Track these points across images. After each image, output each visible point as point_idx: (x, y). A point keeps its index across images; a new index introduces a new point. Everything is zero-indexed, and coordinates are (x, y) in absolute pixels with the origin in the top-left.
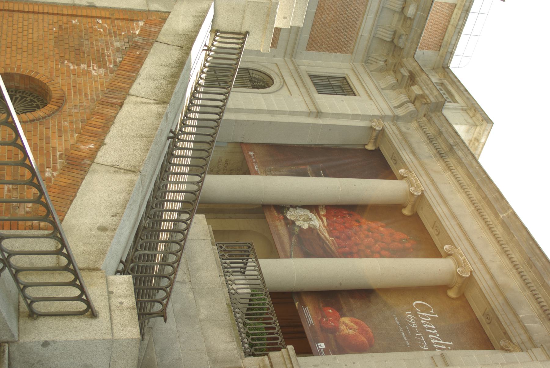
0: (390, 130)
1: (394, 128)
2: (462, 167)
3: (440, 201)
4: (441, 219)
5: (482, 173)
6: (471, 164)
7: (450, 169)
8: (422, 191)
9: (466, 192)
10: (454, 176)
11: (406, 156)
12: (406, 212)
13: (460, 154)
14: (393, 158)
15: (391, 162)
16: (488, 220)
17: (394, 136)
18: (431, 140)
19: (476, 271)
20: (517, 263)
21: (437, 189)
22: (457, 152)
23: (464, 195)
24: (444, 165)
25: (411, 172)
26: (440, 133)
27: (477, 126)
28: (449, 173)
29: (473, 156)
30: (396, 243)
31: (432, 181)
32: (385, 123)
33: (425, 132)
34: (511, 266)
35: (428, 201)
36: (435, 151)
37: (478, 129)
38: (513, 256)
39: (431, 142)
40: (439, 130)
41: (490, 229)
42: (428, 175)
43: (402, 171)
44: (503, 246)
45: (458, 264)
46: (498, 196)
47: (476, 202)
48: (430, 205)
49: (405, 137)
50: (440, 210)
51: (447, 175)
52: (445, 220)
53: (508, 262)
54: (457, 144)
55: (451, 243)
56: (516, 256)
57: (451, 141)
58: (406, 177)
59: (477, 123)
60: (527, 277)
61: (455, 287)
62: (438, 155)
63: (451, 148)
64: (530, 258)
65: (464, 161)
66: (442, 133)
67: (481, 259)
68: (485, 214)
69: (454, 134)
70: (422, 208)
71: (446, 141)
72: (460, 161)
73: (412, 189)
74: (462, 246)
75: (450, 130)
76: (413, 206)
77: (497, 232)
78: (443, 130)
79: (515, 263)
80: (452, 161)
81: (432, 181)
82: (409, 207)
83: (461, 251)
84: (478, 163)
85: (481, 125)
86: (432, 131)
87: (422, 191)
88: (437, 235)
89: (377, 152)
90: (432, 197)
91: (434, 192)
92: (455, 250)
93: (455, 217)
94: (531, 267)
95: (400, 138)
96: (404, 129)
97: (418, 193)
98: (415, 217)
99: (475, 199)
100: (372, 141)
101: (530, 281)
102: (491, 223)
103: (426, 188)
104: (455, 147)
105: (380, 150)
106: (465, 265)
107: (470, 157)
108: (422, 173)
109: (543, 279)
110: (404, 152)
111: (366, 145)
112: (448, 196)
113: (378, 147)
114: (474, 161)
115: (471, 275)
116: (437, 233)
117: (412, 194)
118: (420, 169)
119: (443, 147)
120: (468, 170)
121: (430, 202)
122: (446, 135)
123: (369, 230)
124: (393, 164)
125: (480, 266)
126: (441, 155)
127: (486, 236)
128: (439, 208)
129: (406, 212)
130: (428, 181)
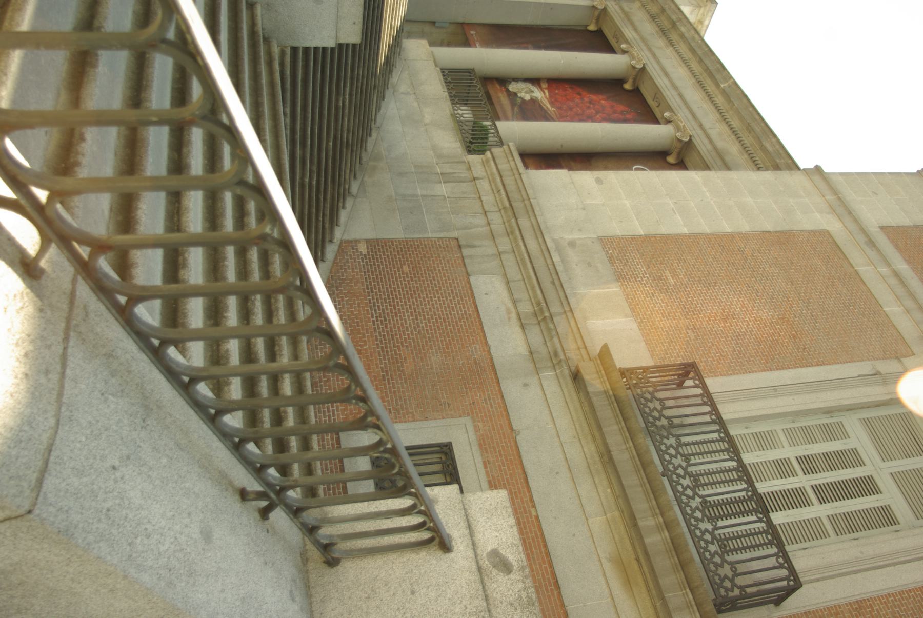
0: (613, 9)
1: (617, 7)
2: (684, 42)
3: (661, 73)
4: (662, 90)
5: (704, 47)
6: (693, 38)
7: (671, 44)
8: (644, 64)
9: (687, 66)
10: (676, 51)
11: (628, 33)
12: (627, 86)
13: (683, 29)
14: (615, 37)
15: (613, 42)
16: (709, 91)
17: (616, 14)
18: (653, 18)
19: (696, 136)
20: (737, 129)
21: (658, 62)
22: (679, 27)
23: (685, 68)
24: (667, 41)
25: (632, 47)
26: (663, 10)
27: (701, 7)
28: (671, 48)
29: (696, 30)
30: (617, 115)
31: (654, 56)
32: (608, 3)
33: (647, 11)
34: (730, 132)
35: (649, 74)
36: (657, 29)
37: (702, 10)
38: (732, 123)
39: (654, 20)
40: (662, 7)
41: (711, 98)
42: (650, 50)
43: (623, 46)
44: (723, 114)
45: (678, 129)
46: (720, 67)
47: (698, 74)
48: (651, 78)
49: (627, 16)
50: (661, 82)
51: (669, 51)
52: (666, 90)
53: (727, 128)
54: (680, 20)
55: (670, 109)
56: (736, 123)
57: (674, 18)
58: (627, 52)
59: (701, 4)
60: (745, 142)
61: (674, 152)
62: (660, 33)
63: (674, 24)
64: (749, 124)
65: (686, 35)
66: (665, 11)
67: (701, 125)
68: (706, 85)
69: (677, 11)
70: (643, 82)
71: (669, 18)
72: (682, 36)
73: (633, 62)
74: (682, 115)
75: (673, 6)
76: (635, 80)
77: (718, 102)
78: (666, 7)
79: (734, 129)
80: (674, 37)
81: (654, 56)
82: (630, 81)
83: (681, 118)
84: (703, 41)
85: (705, 6)
86: (654, 9)
87: (644, 64)
88: (658, 106)
89: (599, 33)
90: (653, 70)
91: (656, 65)
92: (675, 117)
93: (675, 88)
94: (750, 132)
95: (622, 16)
96: (626, 9)
97: (639, 66)
98: (636, 92)
99: (696, 71)
100: (594, 21)
101: (748, 145)
102: (712, 93)
103: (648, 62)
104: (677, 23)
105: (602, 31)
106: (684, 131)
107: (693, 32)
108: (644, 48)
109: (761, 142)
110: (626, 29)
111: (588, 26)
112: (669, 69)
113: (601, 29)
114: (696, 36)
115: (690, 140)
116: (657, 105)
117: (634, 67)
118: (642, 44)
119: (666, 24)
120: (689, 43)
121: (651, 74)
122: (669, 12)
123: (590, 102)
124: (615, 43)
125: (700, 132)
126: (664, 33)
127: (707, 106)
128: (659, 80)
129: (627, 86)
130: (649, 55)
